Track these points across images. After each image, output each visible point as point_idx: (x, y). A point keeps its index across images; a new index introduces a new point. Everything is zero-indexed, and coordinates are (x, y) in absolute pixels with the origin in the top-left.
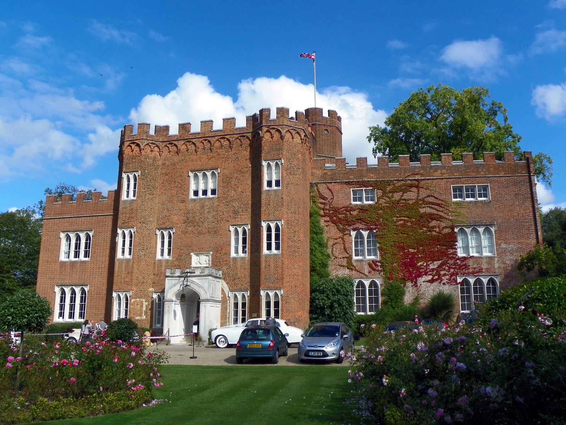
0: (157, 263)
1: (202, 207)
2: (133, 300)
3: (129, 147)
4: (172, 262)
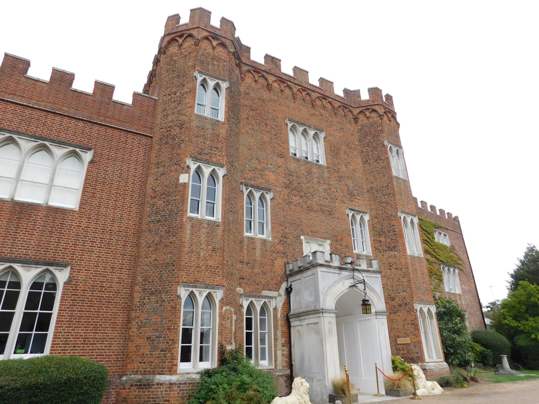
1: (310, 173)
2: (224, 308)
3: (205, 41)
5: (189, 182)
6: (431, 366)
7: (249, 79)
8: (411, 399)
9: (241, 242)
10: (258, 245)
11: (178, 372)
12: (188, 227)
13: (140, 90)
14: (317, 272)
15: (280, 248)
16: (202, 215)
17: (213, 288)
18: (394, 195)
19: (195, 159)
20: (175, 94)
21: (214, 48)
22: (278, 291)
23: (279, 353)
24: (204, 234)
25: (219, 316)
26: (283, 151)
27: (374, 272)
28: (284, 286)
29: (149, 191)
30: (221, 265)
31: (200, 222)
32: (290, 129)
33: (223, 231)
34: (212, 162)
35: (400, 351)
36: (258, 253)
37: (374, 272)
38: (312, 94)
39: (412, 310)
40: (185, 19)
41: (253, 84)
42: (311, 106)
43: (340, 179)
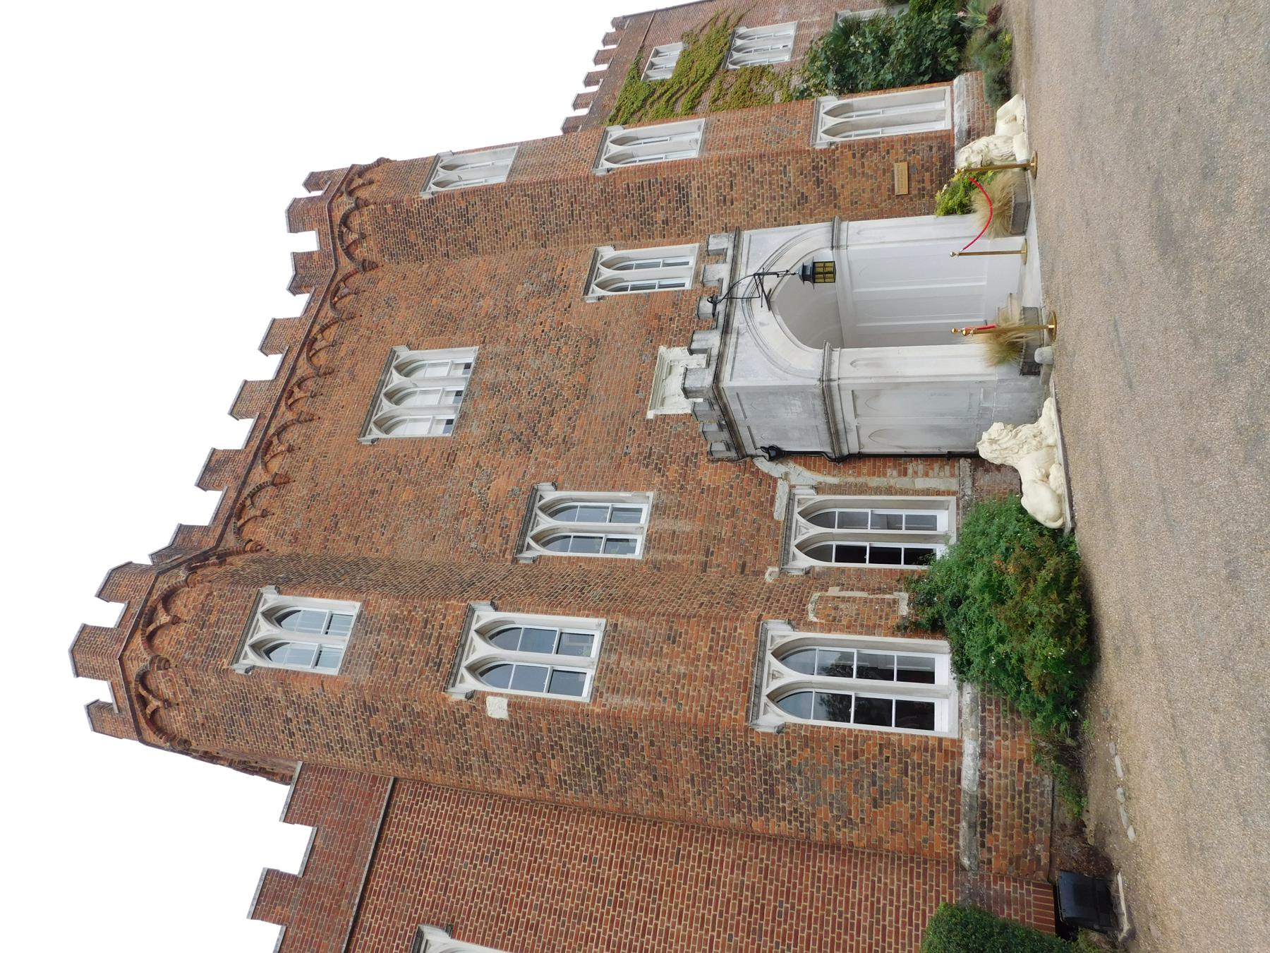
0: (659, 557)
1: (494, 389)
2: (812, 617)
3: (157, 641)
4: (666, 487)
5: (507, 696)
6: (962, 118)
7: (259, 532)
8: (1035, 177)
9: (656, 566)
10: (666, 526)
11: (956, 736)
12: (614, 700)
13: (281, 792)
14: (733, 388)
15: (673, 471)
16: (587, 665)
17: (764, 644)
18: (555, 183)
19: (451, 677)
20: (288, 721)
21: (176, 621)
22: (775, 480)
23: (921, 483)
24: (633, 663)
25: (829, 631)
26: (439, 454)
27: (736, 246)
28: (764, 465)
29: (526, 791)
30: (709, 622)
31: (604, 670)
32: (387, 431)
33: (628, 614)
34: (460, 635)
35: (924, 189)
36: (684, 526)
37: (736, 246)
38: (299, 373)
39: (830, 154)
40: (101, 691)
41: (271, 521)
42: (329, 380)
43: (511, 313)
